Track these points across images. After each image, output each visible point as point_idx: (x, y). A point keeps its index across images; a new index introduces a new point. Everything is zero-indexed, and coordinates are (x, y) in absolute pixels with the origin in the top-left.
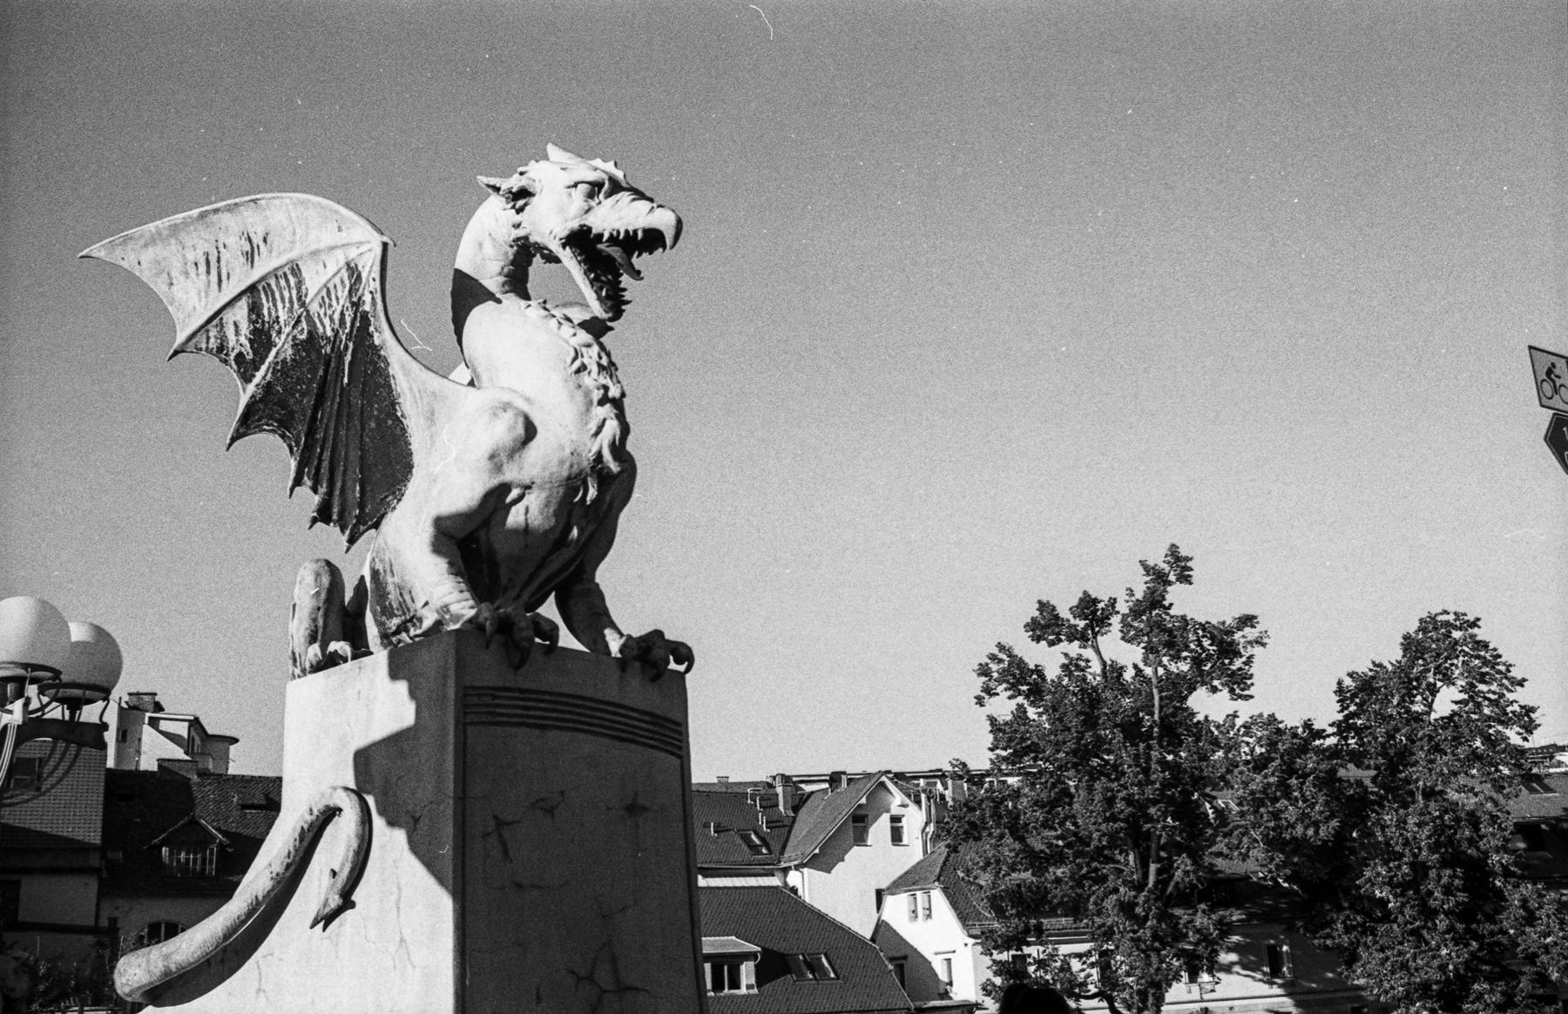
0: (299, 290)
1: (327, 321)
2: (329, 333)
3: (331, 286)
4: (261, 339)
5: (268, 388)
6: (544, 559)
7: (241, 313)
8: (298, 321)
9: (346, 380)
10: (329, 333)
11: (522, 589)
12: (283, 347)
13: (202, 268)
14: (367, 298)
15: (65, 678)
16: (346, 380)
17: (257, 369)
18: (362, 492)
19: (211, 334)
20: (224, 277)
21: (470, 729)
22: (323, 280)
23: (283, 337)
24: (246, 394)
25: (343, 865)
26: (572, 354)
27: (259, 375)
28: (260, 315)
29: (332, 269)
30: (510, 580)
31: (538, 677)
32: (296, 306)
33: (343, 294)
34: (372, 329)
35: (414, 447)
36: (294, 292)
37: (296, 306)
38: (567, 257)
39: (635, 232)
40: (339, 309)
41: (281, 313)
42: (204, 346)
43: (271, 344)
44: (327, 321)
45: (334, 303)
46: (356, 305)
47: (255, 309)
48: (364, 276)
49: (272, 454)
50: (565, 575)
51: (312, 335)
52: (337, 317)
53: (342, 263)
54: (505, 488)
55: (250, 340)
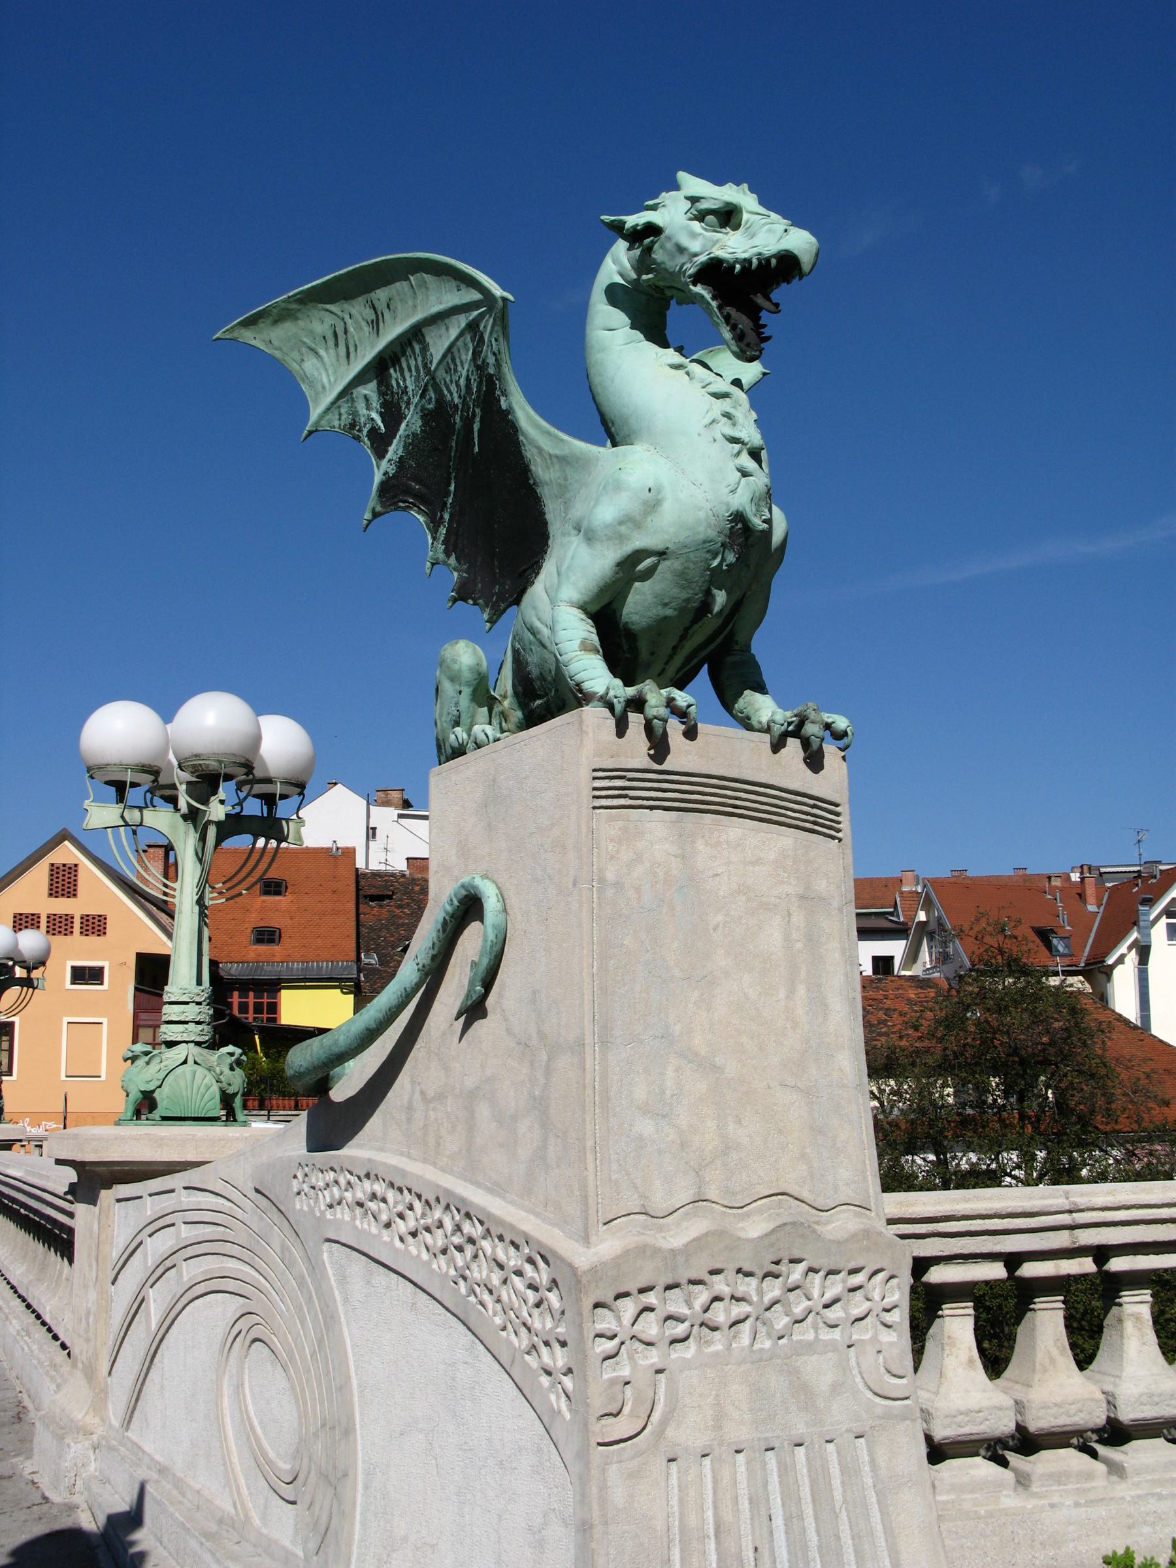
0: (424, 358)
1: (453, 388)
4: (392, 413)
5: (401, 463)
6: (687, 630)
8: (425, 391)
9: (476, 449)
10: (456, 400)
11: (667, 663)
12: (412, 422)
13: (331, 343)
14: (491, 360)
15: (258, 773)
16: (476, 449)
17: (390, 444)
19: (343, 411)
20: (352, 349)
22: (447, 344)
23: (412, 408)
24: (381, 470)
25: (481, 956)
27: (391, 449)
28: (389, 386)
29: (454, 333)
30: (652, 654)
34: (498, 393)
35: (549, 517)
36: (420, 359)
39: (768, 260)
40: (464, 373)
43: (400, 417)
44: (453, 388)
45: (459, 368)
46: (478, 368)
50: (712, 646)
52: (462, 382)
55: (381, 414)
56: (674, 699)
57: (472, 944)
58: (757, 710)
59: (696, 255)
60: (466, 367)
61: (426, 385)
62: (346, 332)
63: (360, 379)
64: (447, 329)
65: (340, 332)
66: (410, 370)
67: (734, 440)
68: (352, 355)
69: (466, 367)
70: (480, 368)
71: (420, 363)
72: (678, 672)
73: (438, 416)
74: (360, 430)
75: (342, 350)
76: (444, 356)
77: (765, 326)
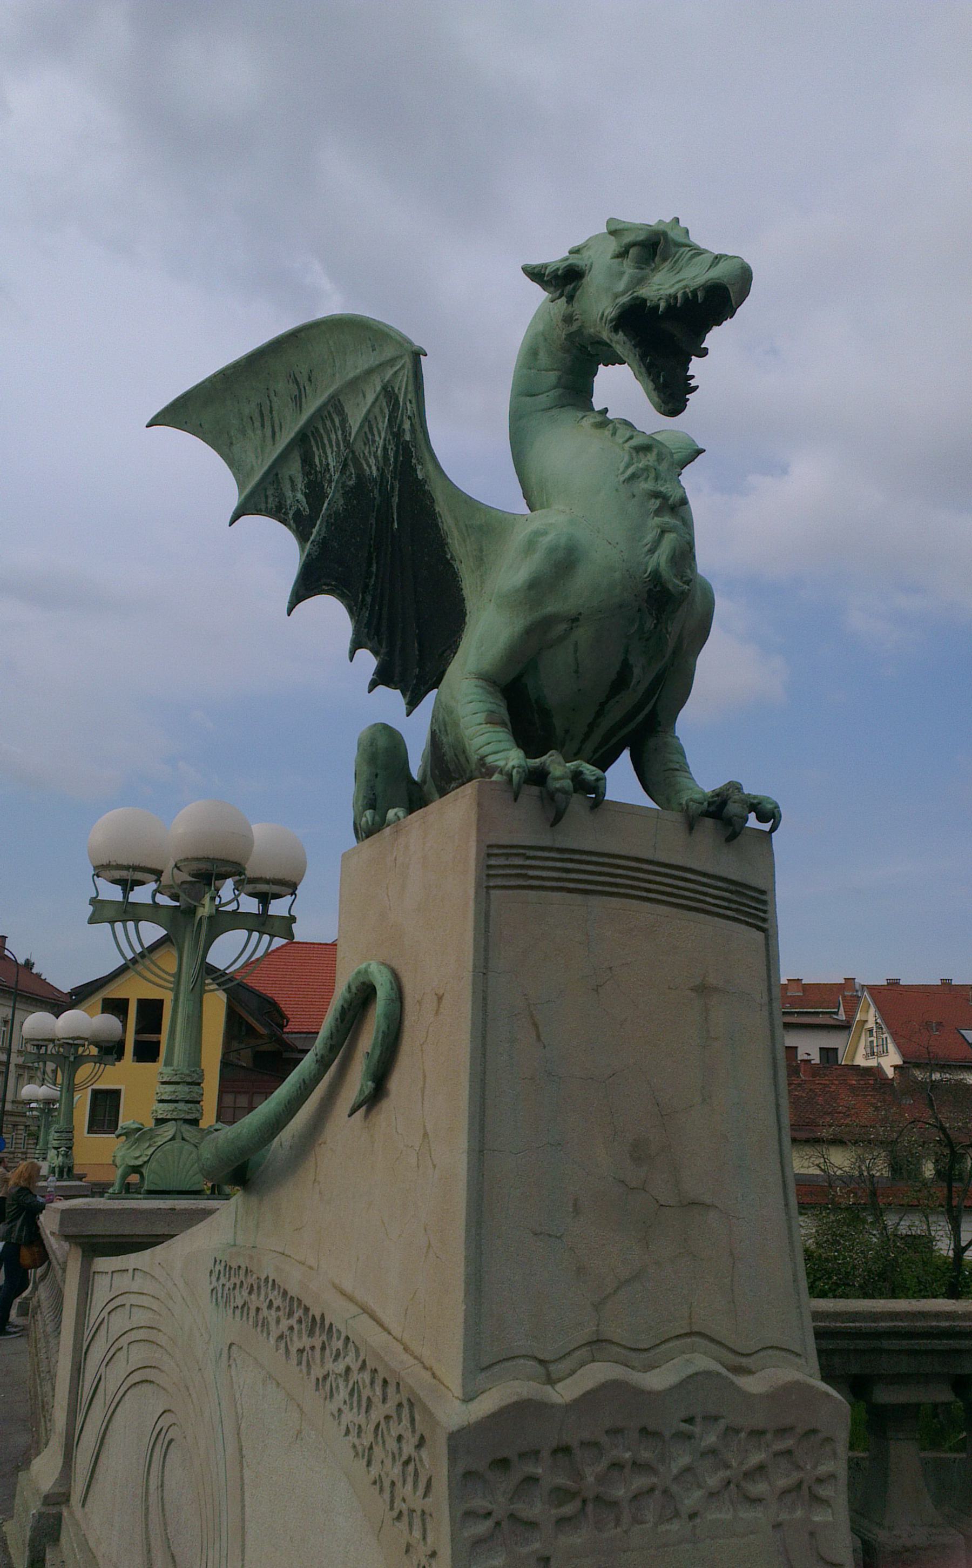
1: (372, 461)
2: (375, 473)
3: (371, 417)
4: (315, 492)
6: (602, 705)
7: (295, 468)
8: (345, 465)
11: (583, 741)
13: (257, 424)
14: (407, 426)
18: (419, 644)
19: (269, 493)
20: (277, 429)
21: (493, 893)
23: (333, 484)
26: (626, 459)
27: (315, 531)
30: (567, 731)
31: (582, 833)
32: (342, 447)
33: (383, 424)
34: (414, 461)
36: (340, 433)
37: (342, 447)
38: (620, 342)
40: (381, 442)
41: (330, 460)
42: (263, 506)
44: (372, 461)
45: (377, 438)
47: (307, 460)
48: (401, 400)
49: (330, 615)
50: (632, 726)
51: (360, 477)
53: (378, 388)
54: (546, 623)
55: (306, 495)
56: (581, 773)
57: (368, 1039)
58: (679, 792)
59: (616, 296)
60: (383, 435)
61: (346, 459)
62: (271, 412)
63: (283, 457)
64: (364, 396)
65: (266, 412)
66: (331, 446)
67: (656, 495)
68: (278, 435)
69: (383, 435)
70: (397, 435)
71: (340, 437)
72: (595, 752)
73: (357, 491)
74: (286, 514)
75: (268, 432)
76: (361, 427)
77: (693, 377)
